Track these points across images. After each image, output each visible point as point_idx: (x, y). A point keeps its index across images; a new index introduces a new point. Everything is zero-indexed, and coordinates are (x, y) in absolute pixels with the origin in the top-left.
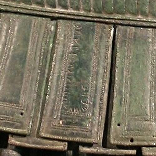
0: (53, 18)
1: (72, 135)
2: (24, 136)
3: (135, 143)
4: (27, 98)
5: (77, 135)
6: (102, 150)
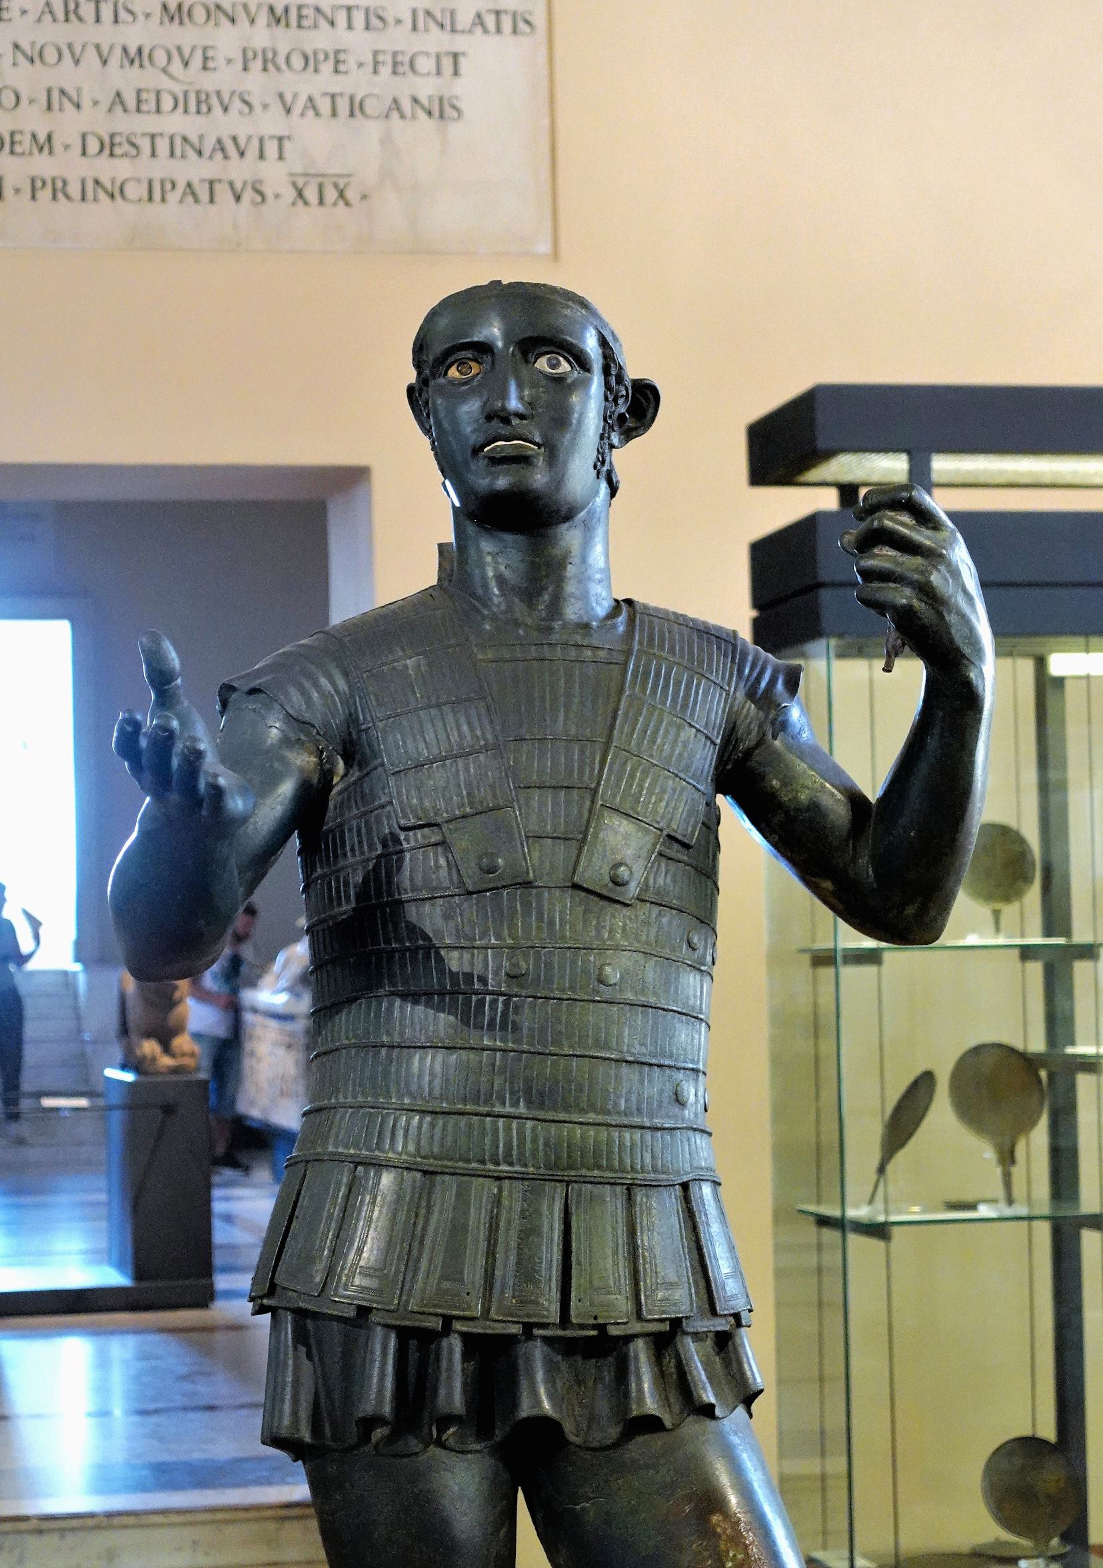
0: (499, 1178)
1: (528, 1316)
2: (472, 1319)
3: (600, 1321)
4: (473, 1274)
5: (535, 1315)
6: (560, 1333)
